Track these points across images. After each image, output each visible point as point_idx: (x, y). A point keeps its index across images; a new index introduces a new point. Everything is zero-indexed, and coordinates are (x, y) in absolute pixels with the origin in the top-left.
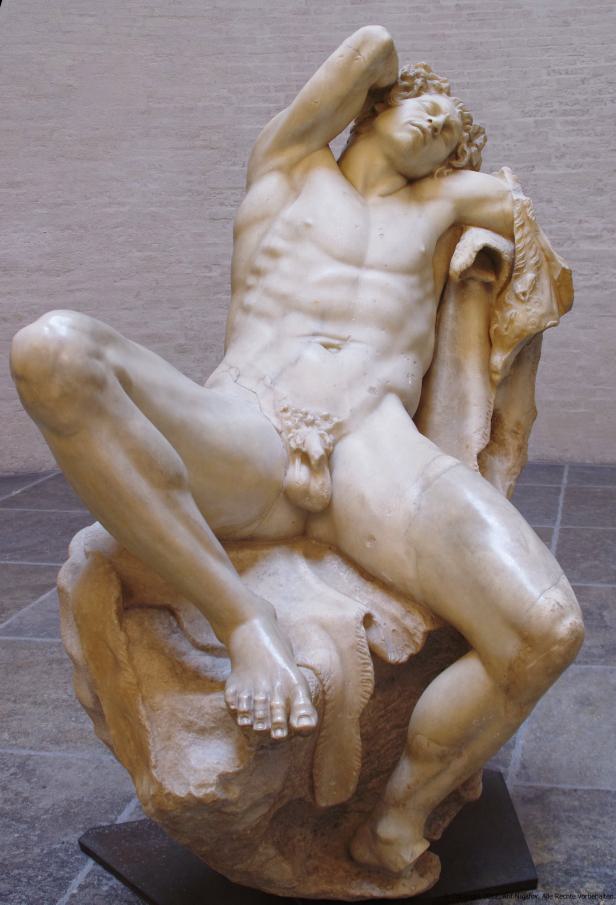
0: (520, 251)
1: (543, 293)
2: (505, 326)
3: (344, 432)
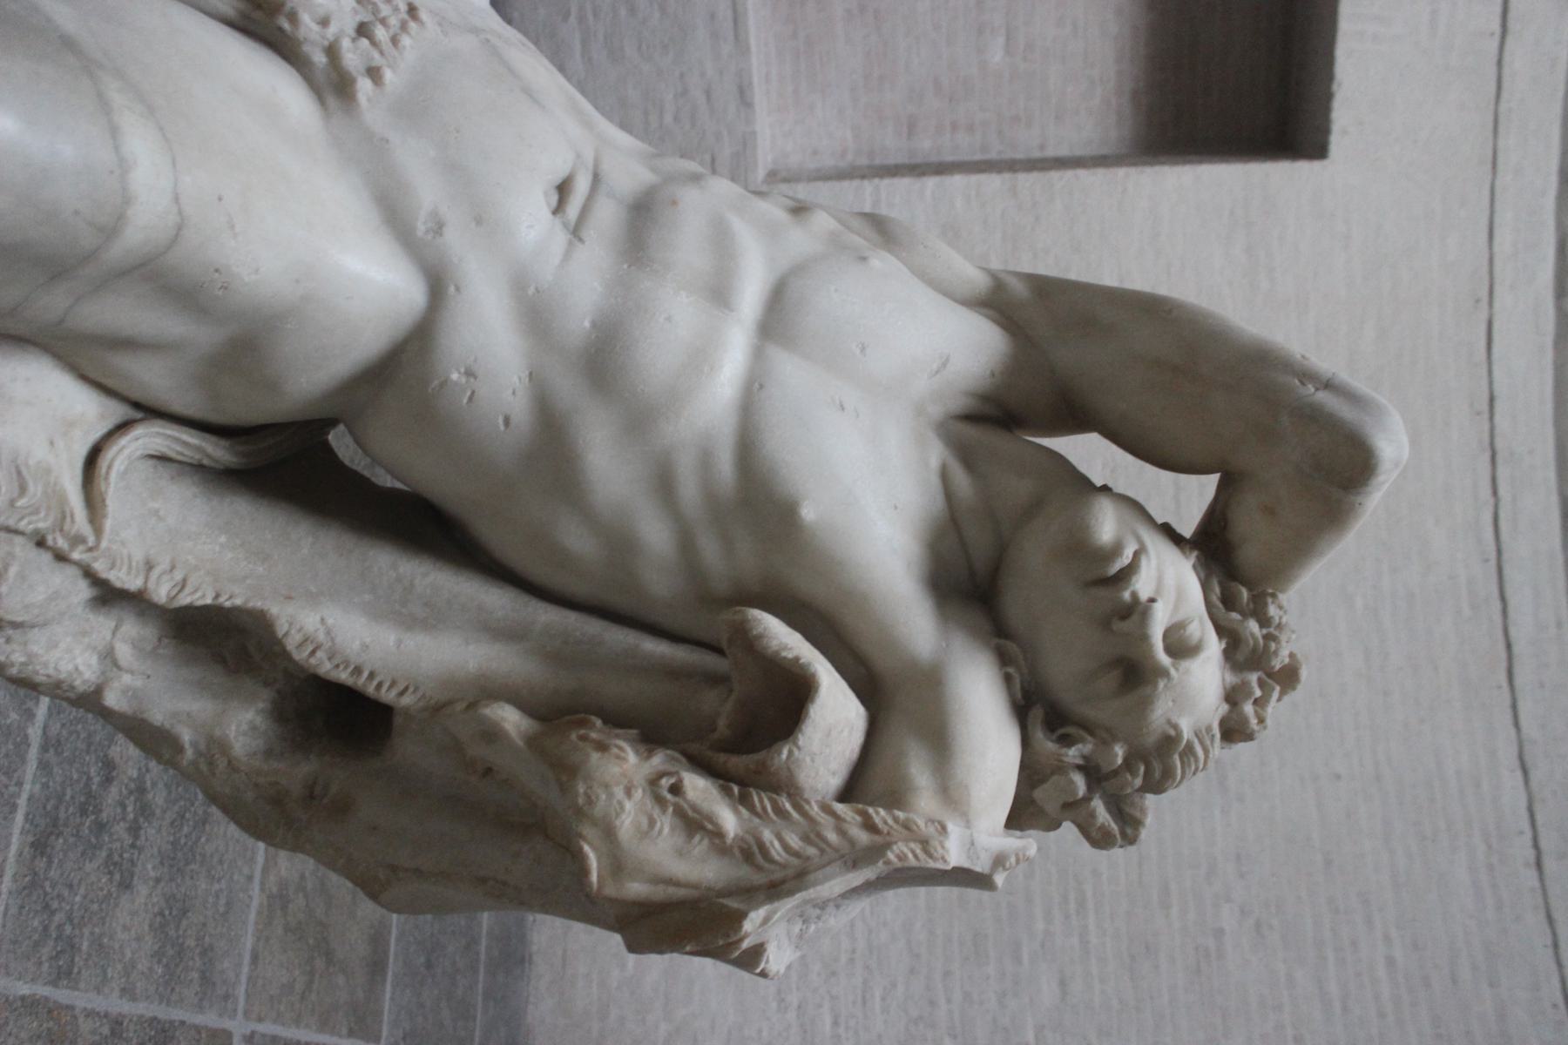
0: (798, 807)
1: (680, 853)
2: (594, 735)
3: (332, 101)
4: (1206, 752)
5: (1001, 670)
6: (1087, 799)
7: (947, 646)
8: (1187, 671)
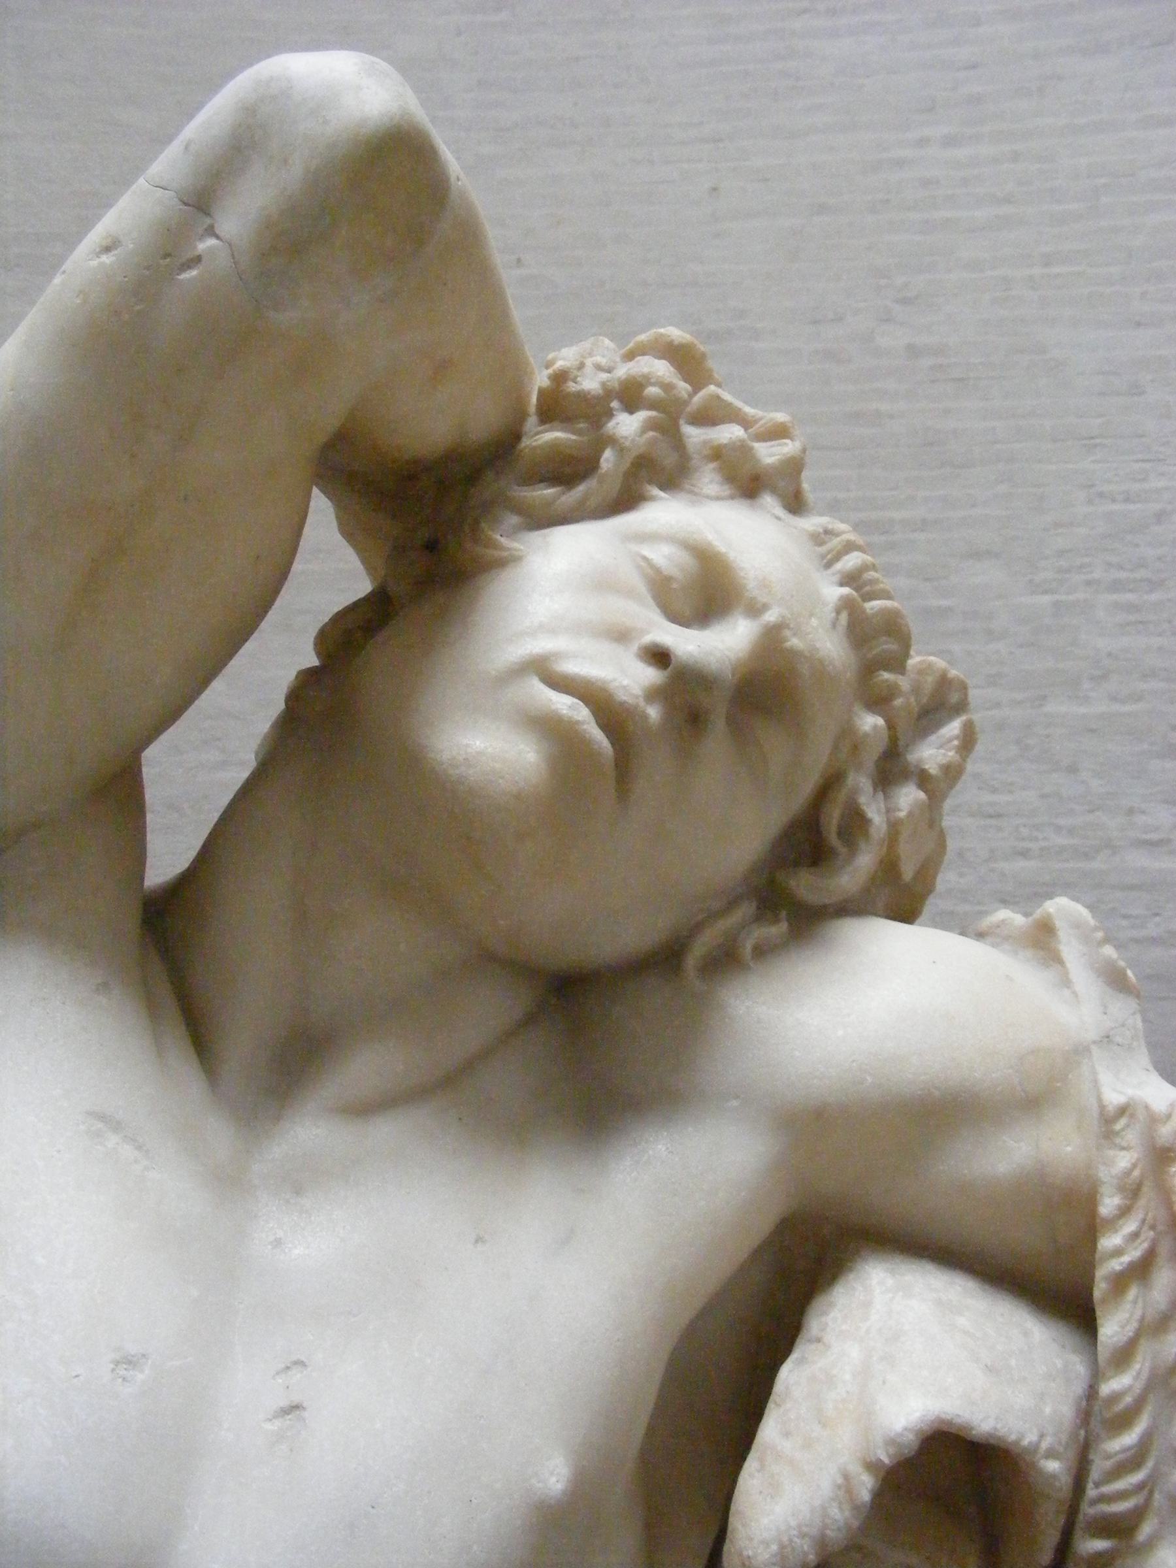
0: (1123, 1421)
4: (849, 547)
5: (749, 968)
6: (923, 779)
7: (737, 1097)
8: (765, 584)
